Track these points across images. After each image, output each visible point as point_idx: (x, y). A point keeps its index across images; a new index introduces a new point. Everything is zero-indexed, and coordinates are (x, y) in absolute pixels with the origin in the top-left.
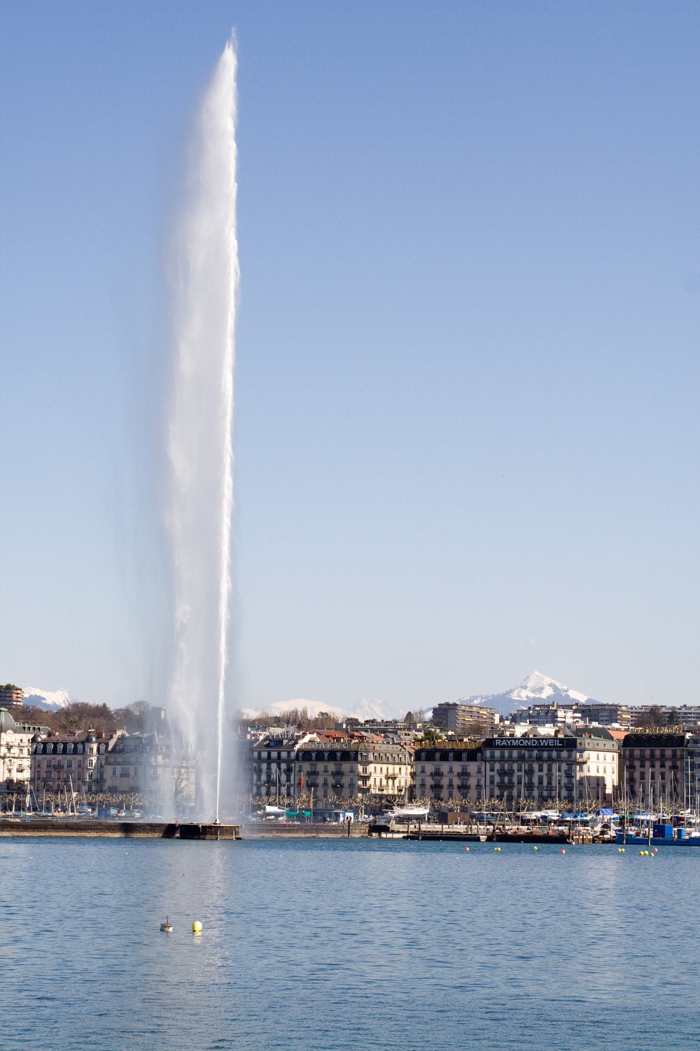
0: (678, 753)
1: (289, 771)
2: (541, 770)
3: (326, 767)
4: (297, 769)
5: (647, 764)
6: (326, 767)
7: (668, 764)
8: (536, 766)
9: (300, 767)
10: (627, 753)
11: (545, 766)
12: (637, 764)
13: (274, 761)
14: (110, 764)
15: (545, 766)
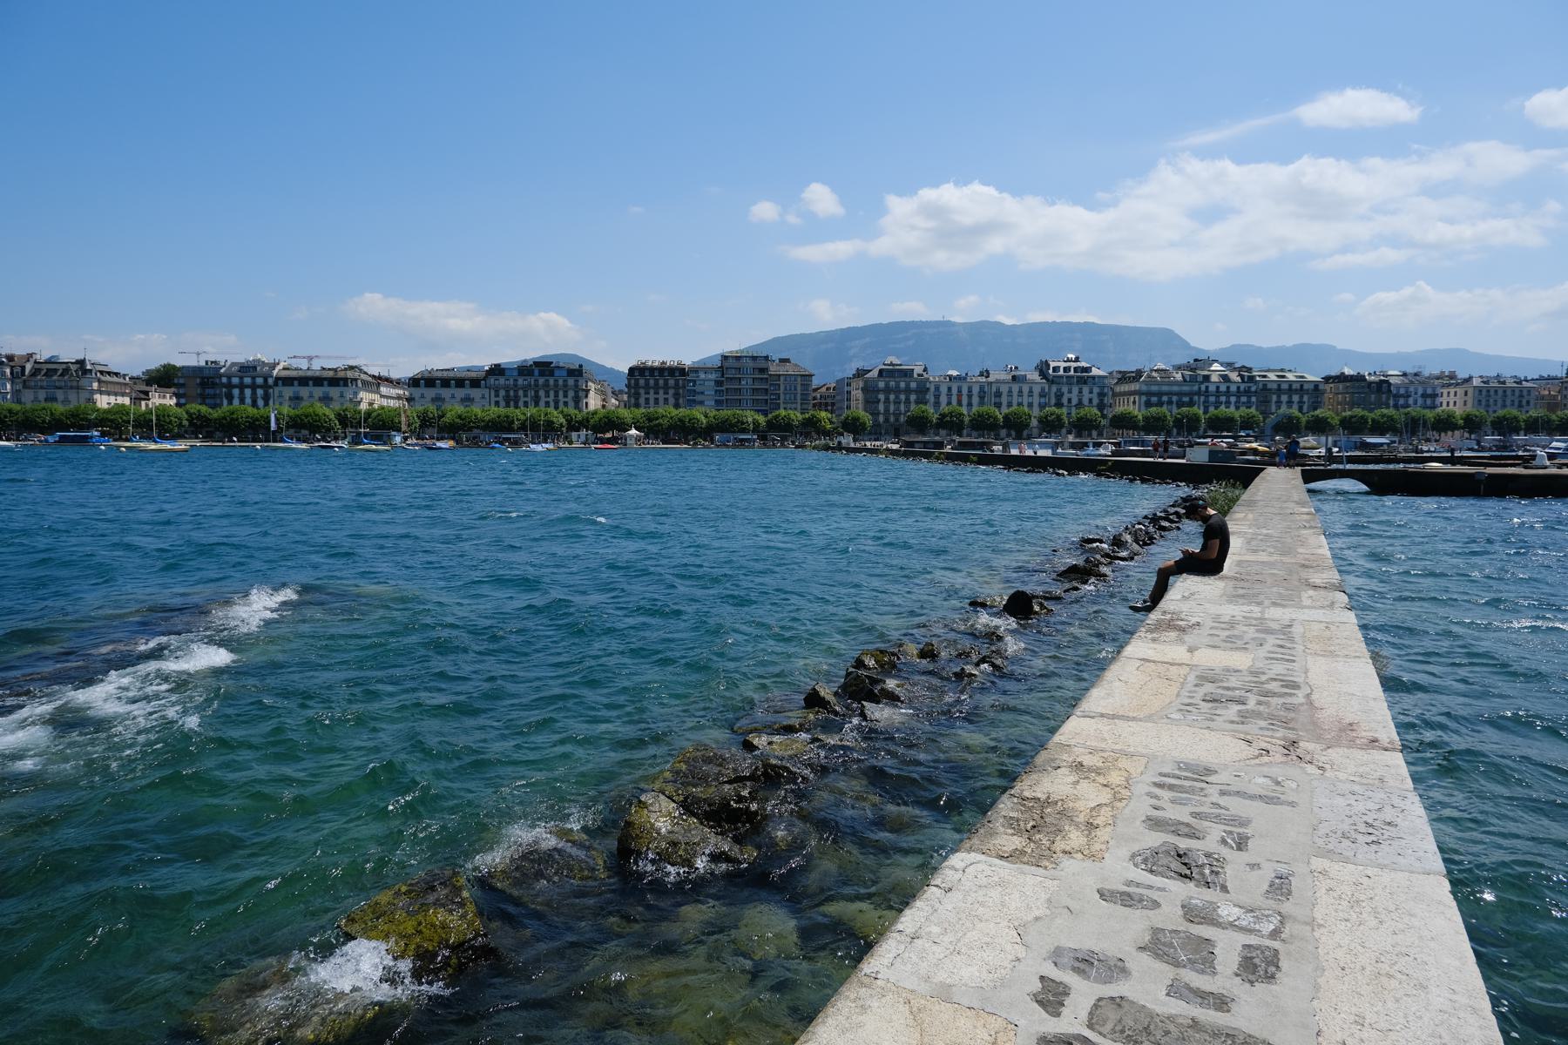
0: (681, 382)
1: (266, 398)
2: (547, 396)
3: (311, 393)
4: (276, 394)
5: (652, 391)
6: (311, 393)
7: (671, 392)
8: (542, 393)
9: (280, 392)
10: (633, 382)
11: (552, 393)
12: (642, 391)
13: (248, 387)
14: (29, 388)
15: (552, 393)
